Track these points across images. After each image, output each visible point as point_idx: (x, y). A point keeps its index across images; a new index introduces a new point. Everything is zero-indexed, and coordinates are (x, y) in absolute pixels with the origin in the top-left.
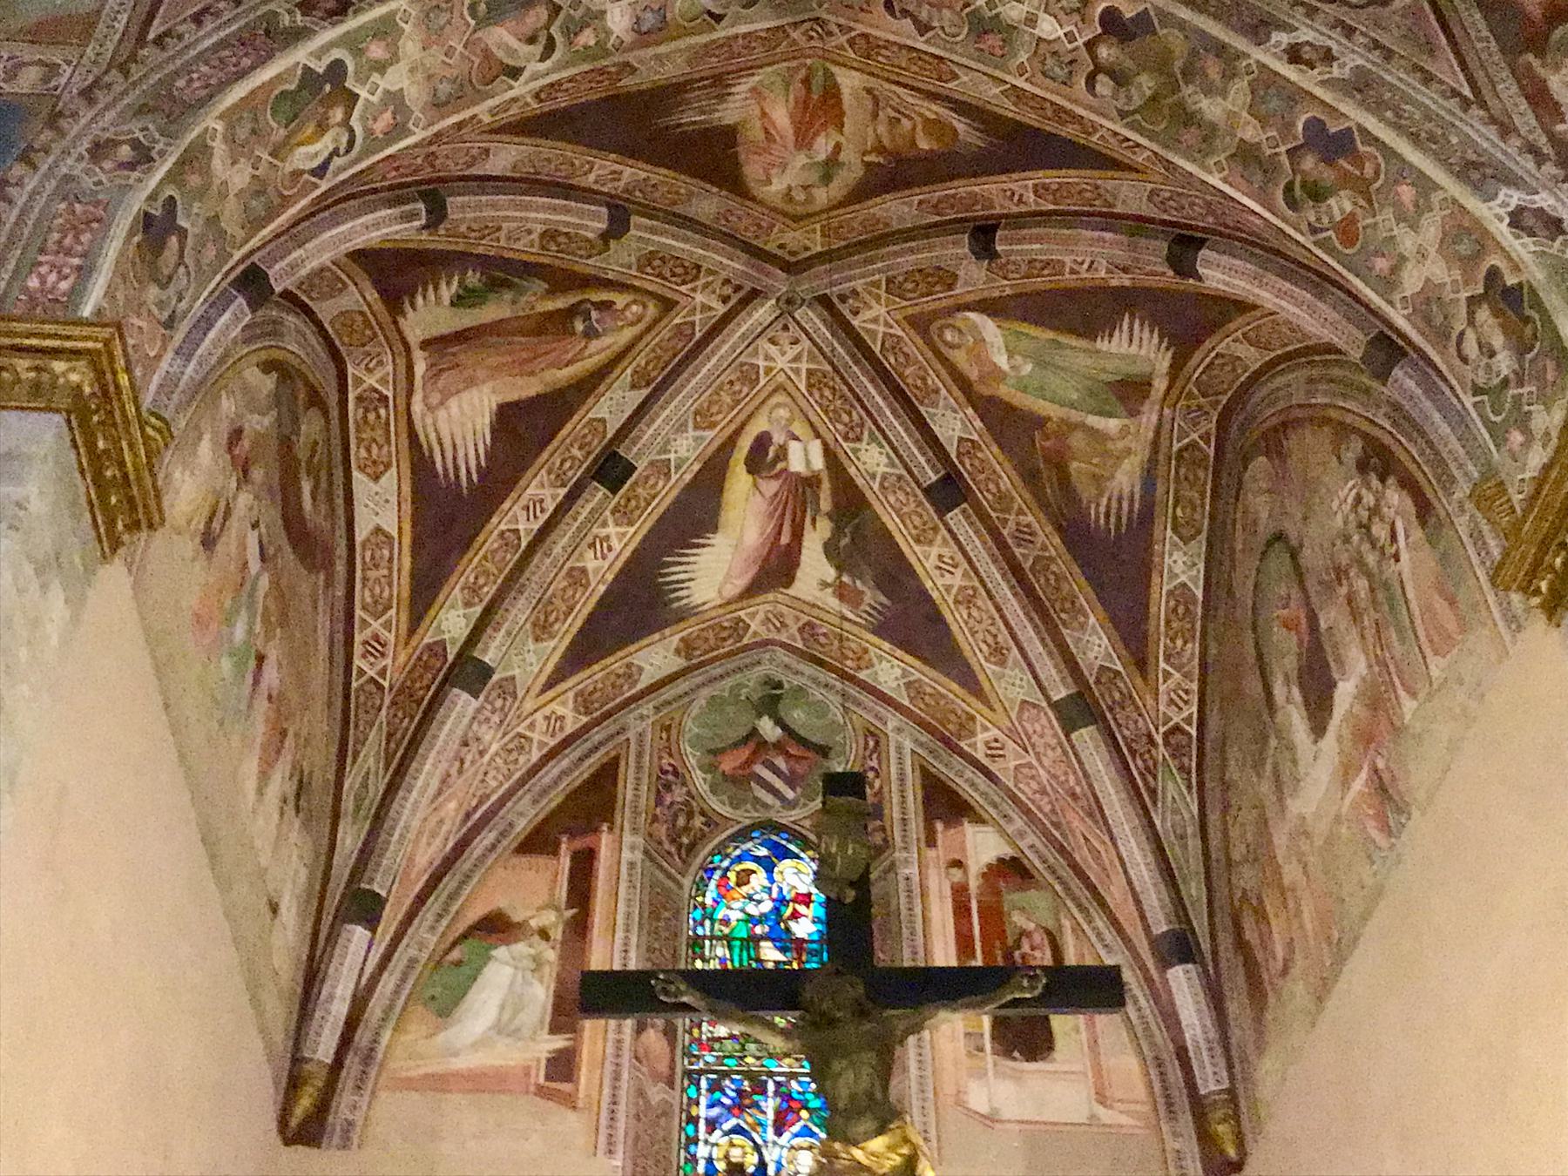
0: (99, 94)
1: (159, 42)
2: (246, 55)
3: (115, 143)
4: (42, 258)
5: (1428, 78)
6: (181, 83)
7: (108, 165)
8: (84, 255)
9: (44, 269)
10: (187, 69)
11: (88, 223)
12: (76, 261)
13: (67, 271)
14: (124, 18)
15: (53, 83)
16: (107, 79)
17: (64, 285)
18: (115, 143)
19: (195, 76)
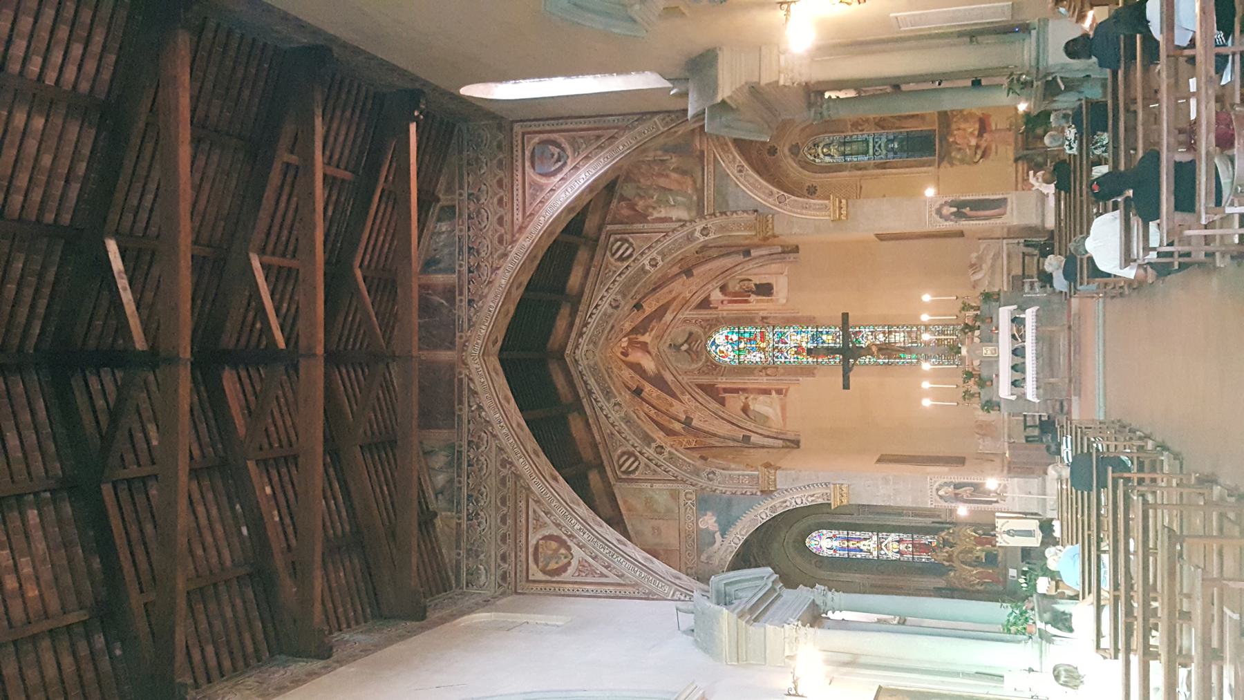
3: (708, 478)
5: (658, 240)
10: (685, 471)
18: (708, 478)
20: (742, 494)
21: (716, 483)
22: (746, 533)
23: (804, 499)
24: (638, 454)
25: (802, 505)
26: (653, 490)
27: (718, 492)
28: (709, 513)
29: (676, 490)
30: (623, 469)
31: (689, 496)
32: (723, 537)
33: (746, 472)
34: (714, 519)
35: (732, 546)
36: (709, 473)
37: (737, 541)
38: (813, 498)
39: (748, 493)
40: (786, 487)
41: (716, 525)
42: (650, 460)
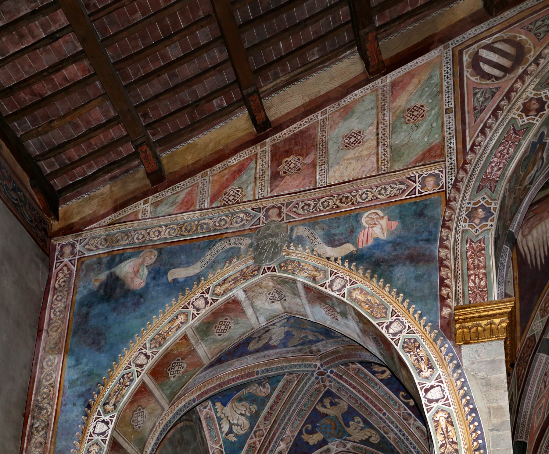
0: (460, 184)
1: (472, 149)
2: (510, 146)
4: (471, 272)
6: (489, 171)
7: (477, 221)
8: (485, 267)
9: (472, 277)
10: (488, 162)
11: (480, 251)
12: (482, 271)
13: (481, 276)
14: (454, 141)
15: (441, 185)
16: (460, 176)
17: (483, 283)
19: (493, 164)
20: (442, 280)
21: (463, 226)
22: (353, 300)
23: (440, 404)
24: (521, 70)
25: (424, 401)
26: (439, 116)
27: (445, 232)
28: (395, 224)
29: (442, 155)
30: (484, 53)
31: (430, 182)
32: (343, 259)
33: (494, 277)
34: (383, 236)
35: (326, 277)
36: (487, 210)
37: (336, 286)
38: (443, 423)
39: (444, 292)
40: (465, 363)
41: (371, 242)
42: (508, 96)
